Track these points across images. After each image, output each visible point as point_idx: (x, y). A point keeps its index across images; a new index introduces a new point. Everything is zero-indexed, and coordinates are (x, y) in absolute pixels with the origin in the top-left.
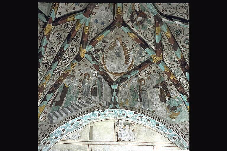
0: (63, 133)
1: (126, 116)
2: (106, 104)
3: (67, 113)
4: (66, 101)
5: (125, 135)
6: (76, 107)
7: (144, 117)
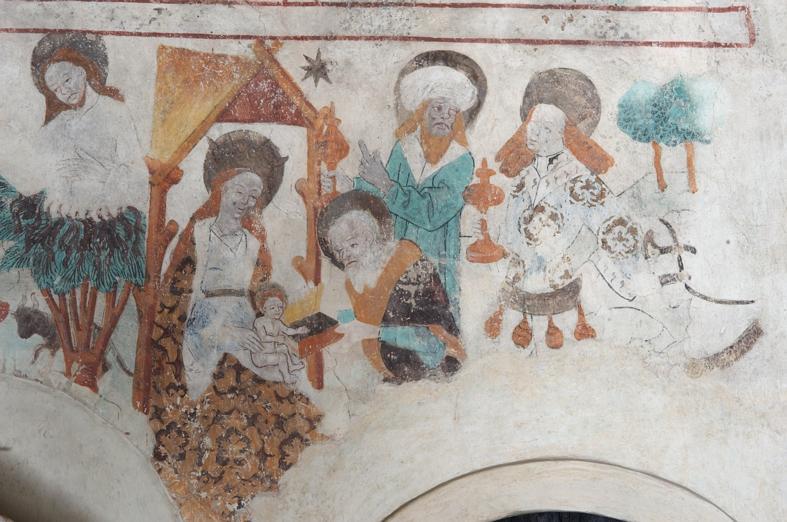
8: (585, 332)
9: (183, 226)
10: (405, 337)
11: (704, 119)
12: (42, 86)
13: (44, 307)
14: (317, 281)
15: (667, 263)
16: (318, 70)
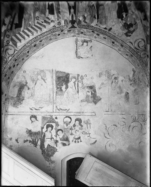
0: (28, 54)
1: (83, 33)
2: (65, 23)
3: (28, 36)
4: (25, 22)
5: (83, 53)
6: (36, 28)
7: (101, 35)
9: (44, 132)
10: (64, 142)
11: (91, 122)
12: (31, 120)
13: (32, 140)
15: (88, 135)
16: (56, 118)
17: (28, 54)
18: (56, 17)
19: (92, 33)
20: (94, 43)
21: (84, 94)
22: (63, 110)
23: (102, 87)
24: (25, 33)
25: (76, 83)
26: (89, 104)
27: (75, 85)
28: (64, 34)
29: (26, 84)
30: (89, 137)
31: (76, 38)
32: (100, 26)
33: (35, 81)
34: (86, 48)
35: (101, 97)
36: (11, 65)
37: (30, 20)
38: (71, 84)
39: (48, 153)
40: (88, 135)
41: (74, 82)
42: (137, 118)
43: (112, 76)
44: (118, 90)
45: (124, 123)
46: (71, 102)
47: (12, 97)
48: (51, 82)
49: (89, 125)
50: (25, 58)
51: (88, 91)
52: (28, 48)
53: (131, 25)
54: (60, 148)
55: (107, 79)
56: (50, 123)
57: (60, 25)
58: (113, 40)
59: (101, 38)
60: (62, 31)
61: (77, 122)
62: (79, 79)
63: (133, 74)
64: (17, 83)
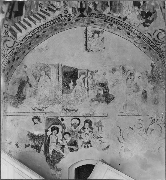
0: (30, 47)
2: (72, 11)
3: (30, 25)
4: (26, 10)
5: (94, 45)
7: (114, 25)
8: (91, 146)
10: (72, 147)
11: (103, 124)
12: (34, 122)
13: (34, 144)
14: (63, 141)
15: (100, 139)
16: (63, 120)
17: (30, 47)
18: (63, 4)
19: (104, 22)
20: (106, 34)
21: (94, 93)
22: (71, 110)
23: (115, 84)
24: (26, 22)
25: (86, 79)
26: (101, 103)
27: (84, 82)
28: (72, 23)
29: (27, 81)
30: (100, 142)
31: (85, 28)
32: (113, 15)
33: (37, 77)
34: (97, 40)
35: (115, 96)
36: (10, 59)
37: (32, 7)
38: (79, 81)
39: (54, 159)
40: (100, 139)
41: (83, 79)
42: (156, 120)
43: (127, 72)
44: (134, 88)
45: (141, 126)
46: (80, 102)
47: (11, 96)
48: (55, 80)
49: (100, 128)
50: (27, 51)
51: (99, 89)
52: (30, 40)
53: (149, 14)
54: (67, 153)
55: (121, 75)
56: (55, 124)
57: (67, 13)
58: (129, 30)
59: (114, 28)
60: (69, 20)
61: (87, 124)
62: (89, 75)
63: (151, 69)
64: (18, 80)
